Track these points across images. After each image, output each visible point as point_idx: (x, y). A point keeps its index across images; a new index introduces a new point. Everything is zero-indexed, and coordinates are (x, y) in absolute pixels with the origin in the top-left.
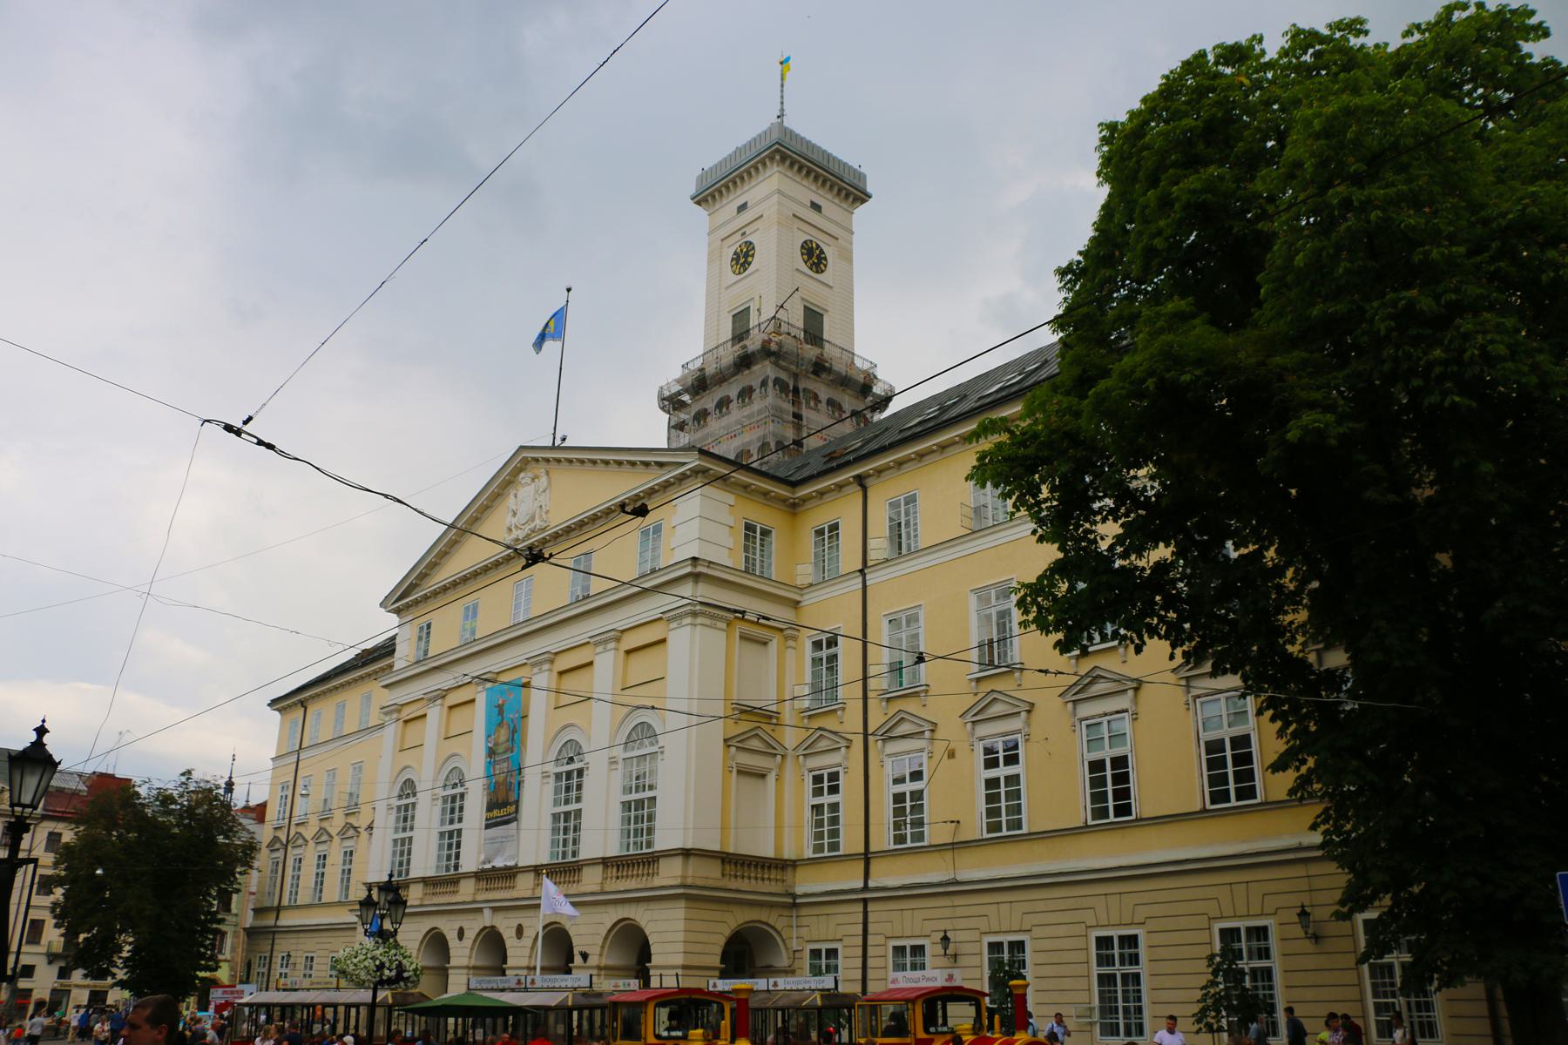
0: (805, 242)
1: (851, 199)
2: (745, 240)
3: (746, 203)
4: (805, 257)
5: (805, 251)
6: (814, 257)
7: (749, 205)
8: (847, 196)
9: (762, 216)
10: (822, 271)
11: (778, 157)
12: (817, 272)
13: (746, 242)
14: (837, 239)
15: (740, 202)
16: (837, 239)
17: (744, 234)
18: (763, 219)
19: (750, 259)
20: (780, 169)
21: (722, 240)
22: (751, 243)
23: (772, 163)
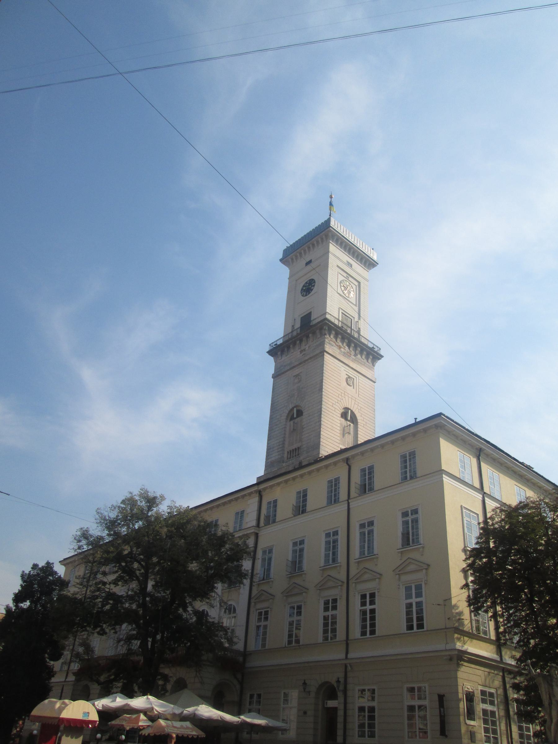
0: (343, 280)
1: (368, 264)
7: (312, 261)
9: (320, 265)
14: (359, 283)
15: (308, 260)
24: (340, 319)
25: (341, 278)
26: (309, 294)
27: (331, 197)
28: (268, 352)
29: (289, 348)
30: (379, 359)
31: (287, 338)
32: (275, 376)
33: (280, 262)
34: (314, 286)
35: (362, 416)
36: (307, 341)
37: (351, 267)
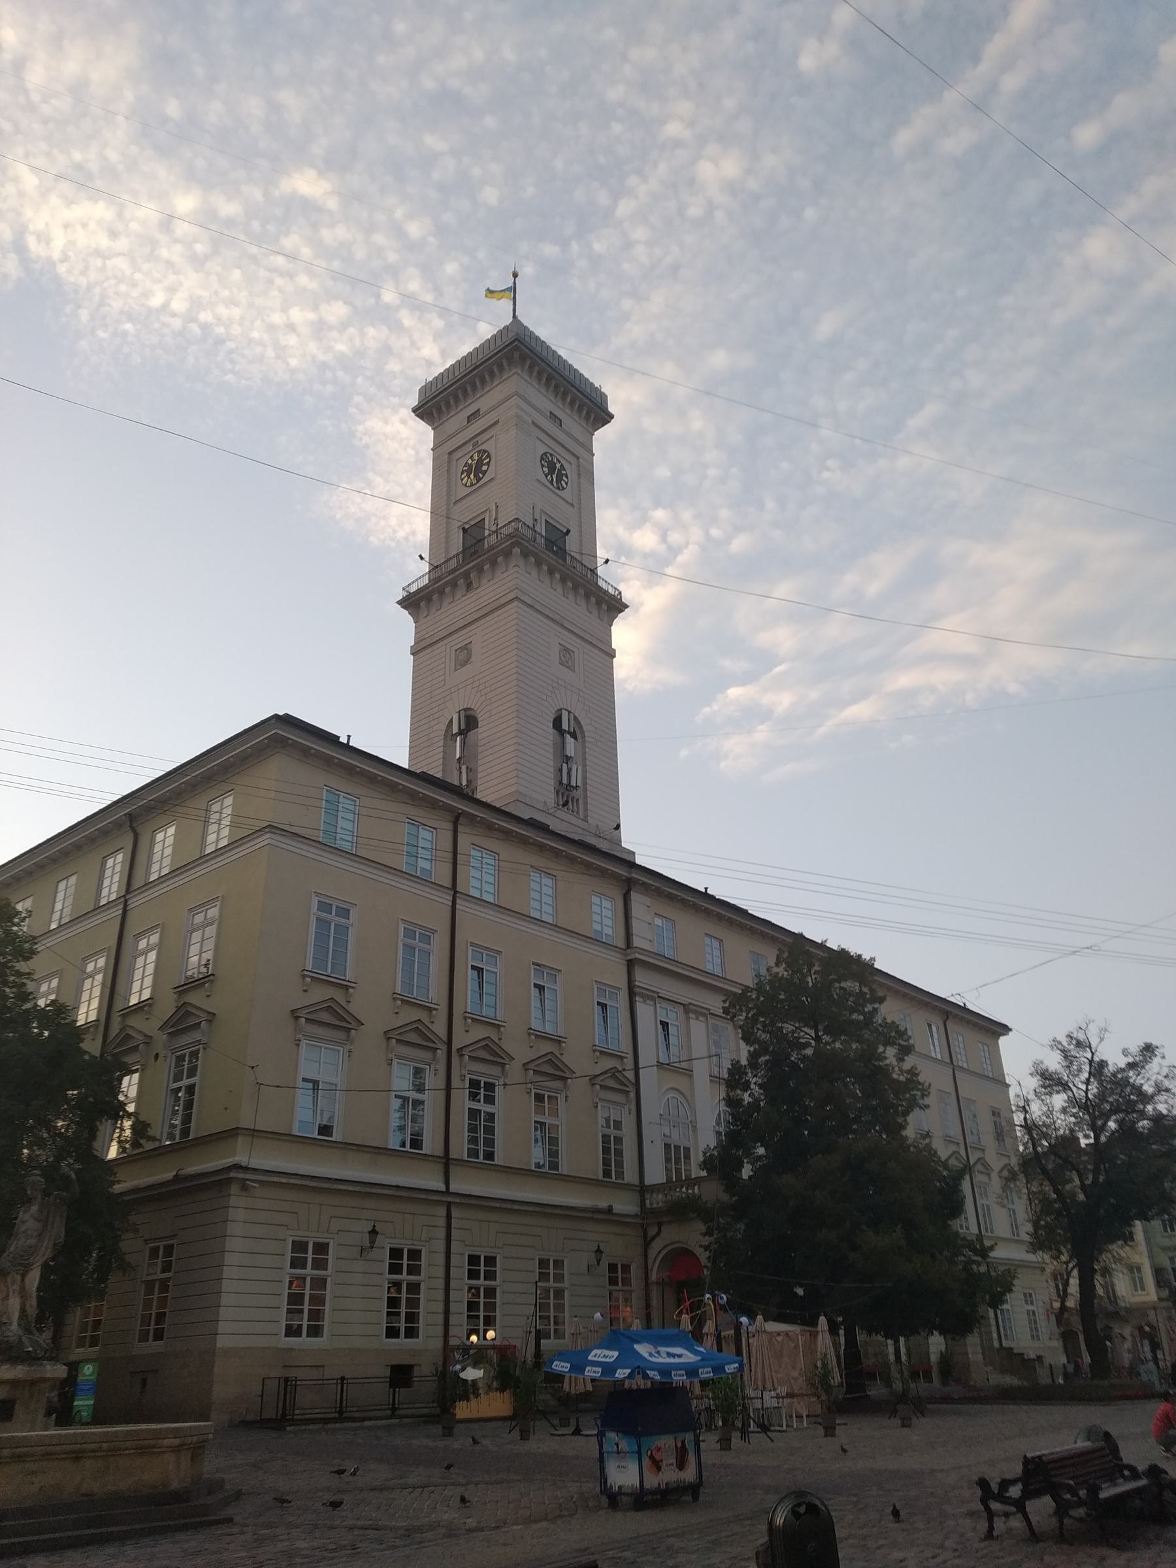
0: (545, 453)
2: (477, 449)
3: (478, 410)
4: (546, 470)
5: (546, 464)
6: (554, 471)
8: (588, 413)
9: (497, 422)
10: (563, 489)
11: (516, 355)
12: (558, 488)
13: (479, 452)
16: (578, 458)
17: (476, 444)
18: (500, 424)
19: (485, 468)
20: (519, 372)
21: (450, 453)
22: (485, 451)
23: (509, 365)
24: (544, 533)
25: (543, 450)
26: (479, 479)
27: (515, 275)
28: (399, 603)
29: (441, 592)
30: (622, 611)
31: (435, 575)
32: (415, 652)
33: (413, 414)
34: (488, 464)
35: (593, 723)
36: (479, 578)
37: (561, 425)
